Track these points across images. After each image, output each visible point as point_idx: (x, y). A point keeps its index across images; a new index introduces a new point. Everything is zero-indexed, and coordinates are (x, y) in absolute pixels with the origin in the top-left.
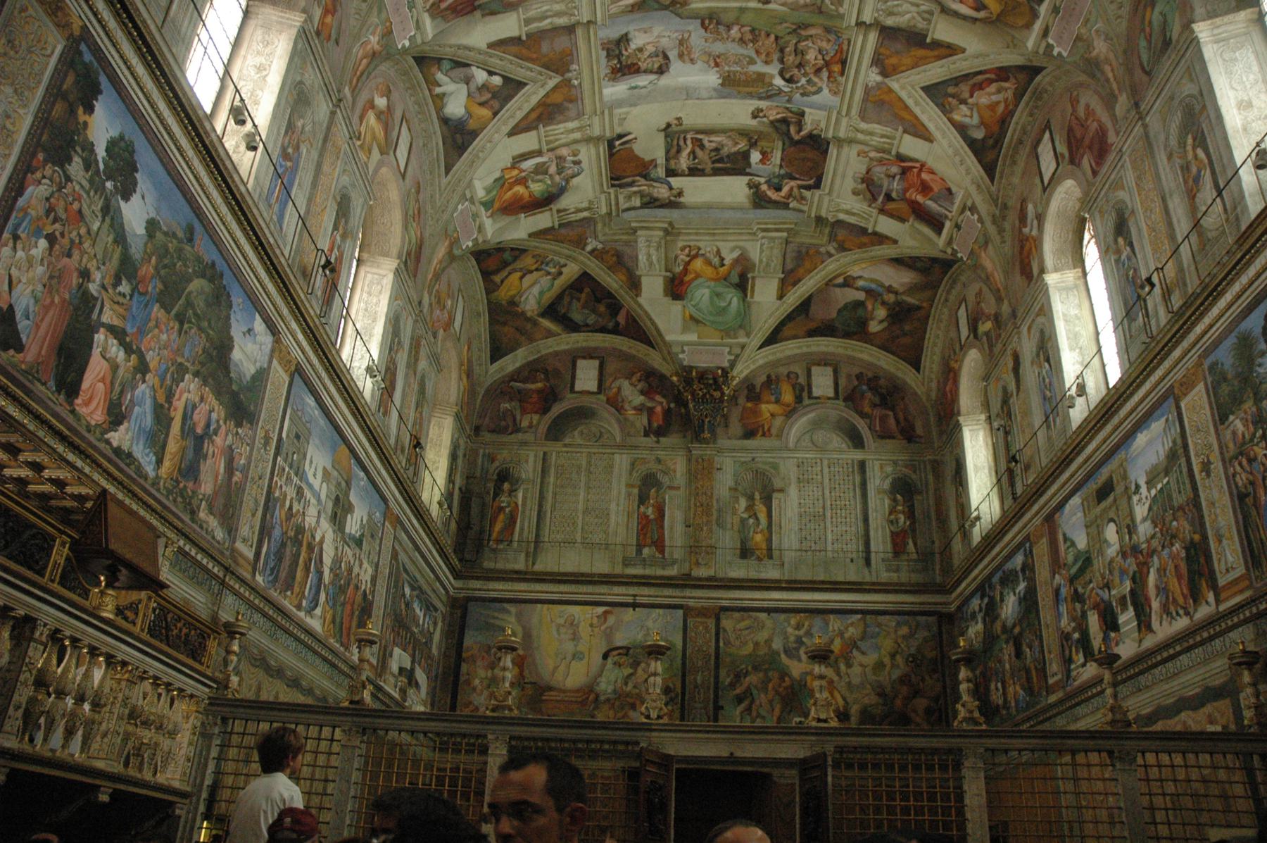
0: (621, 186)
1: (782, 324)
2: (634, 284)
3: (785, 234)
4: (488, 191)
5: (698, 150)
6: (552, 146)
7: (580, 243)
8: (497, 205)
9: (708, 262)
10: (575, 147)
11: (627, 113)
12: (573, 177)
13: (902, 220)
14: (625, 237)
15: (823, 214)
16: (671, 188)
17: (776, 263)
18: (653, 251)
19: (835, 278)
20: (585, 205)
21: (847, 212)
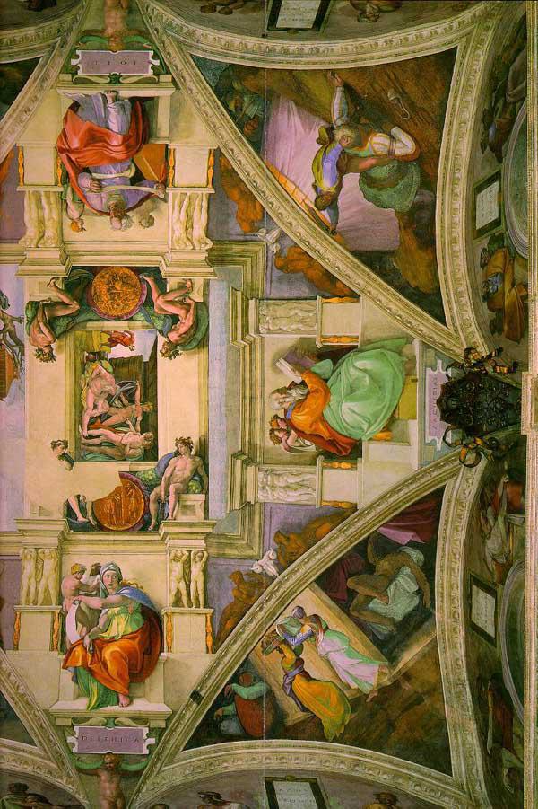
0: (161, 516)
1: (404, 289)
2: (339, 514)
3: (252, 302)
4: (88, 694)
5: (113, 420)
6: (54, 598)
7: (254, 586)
8: (119, 687)
9: (300, 404)
10: (67, 569)
11: (33, 505)
12: (120, 579)
13: (167, 151)
14: (257, 518)
15: (203, 256)
16: (177, 454)
17: (297, 310)
18: (281, 482)
19: (321, 223)
20: (178, 568)
21: (189, 224)
